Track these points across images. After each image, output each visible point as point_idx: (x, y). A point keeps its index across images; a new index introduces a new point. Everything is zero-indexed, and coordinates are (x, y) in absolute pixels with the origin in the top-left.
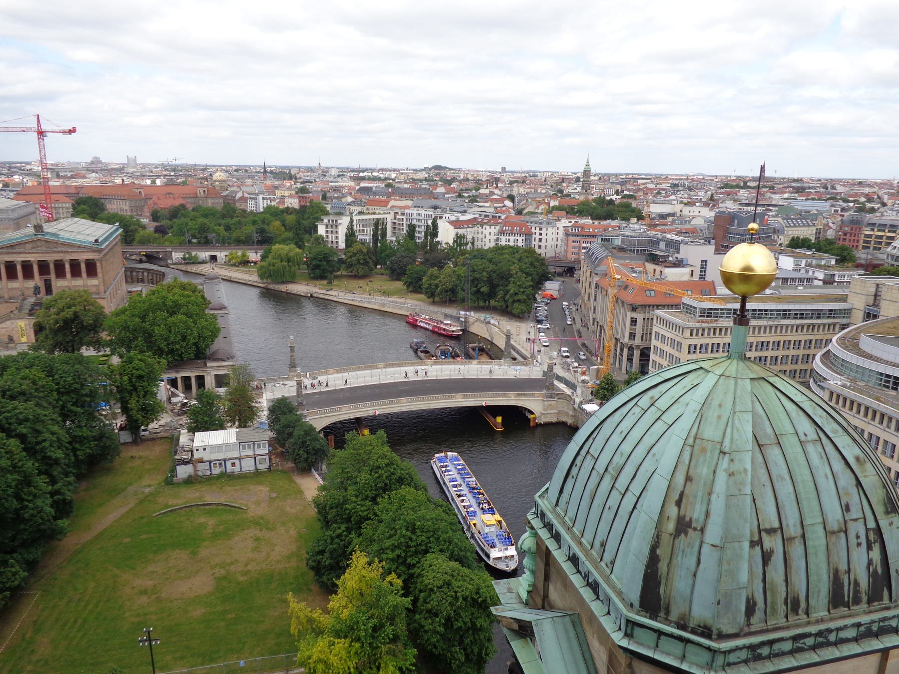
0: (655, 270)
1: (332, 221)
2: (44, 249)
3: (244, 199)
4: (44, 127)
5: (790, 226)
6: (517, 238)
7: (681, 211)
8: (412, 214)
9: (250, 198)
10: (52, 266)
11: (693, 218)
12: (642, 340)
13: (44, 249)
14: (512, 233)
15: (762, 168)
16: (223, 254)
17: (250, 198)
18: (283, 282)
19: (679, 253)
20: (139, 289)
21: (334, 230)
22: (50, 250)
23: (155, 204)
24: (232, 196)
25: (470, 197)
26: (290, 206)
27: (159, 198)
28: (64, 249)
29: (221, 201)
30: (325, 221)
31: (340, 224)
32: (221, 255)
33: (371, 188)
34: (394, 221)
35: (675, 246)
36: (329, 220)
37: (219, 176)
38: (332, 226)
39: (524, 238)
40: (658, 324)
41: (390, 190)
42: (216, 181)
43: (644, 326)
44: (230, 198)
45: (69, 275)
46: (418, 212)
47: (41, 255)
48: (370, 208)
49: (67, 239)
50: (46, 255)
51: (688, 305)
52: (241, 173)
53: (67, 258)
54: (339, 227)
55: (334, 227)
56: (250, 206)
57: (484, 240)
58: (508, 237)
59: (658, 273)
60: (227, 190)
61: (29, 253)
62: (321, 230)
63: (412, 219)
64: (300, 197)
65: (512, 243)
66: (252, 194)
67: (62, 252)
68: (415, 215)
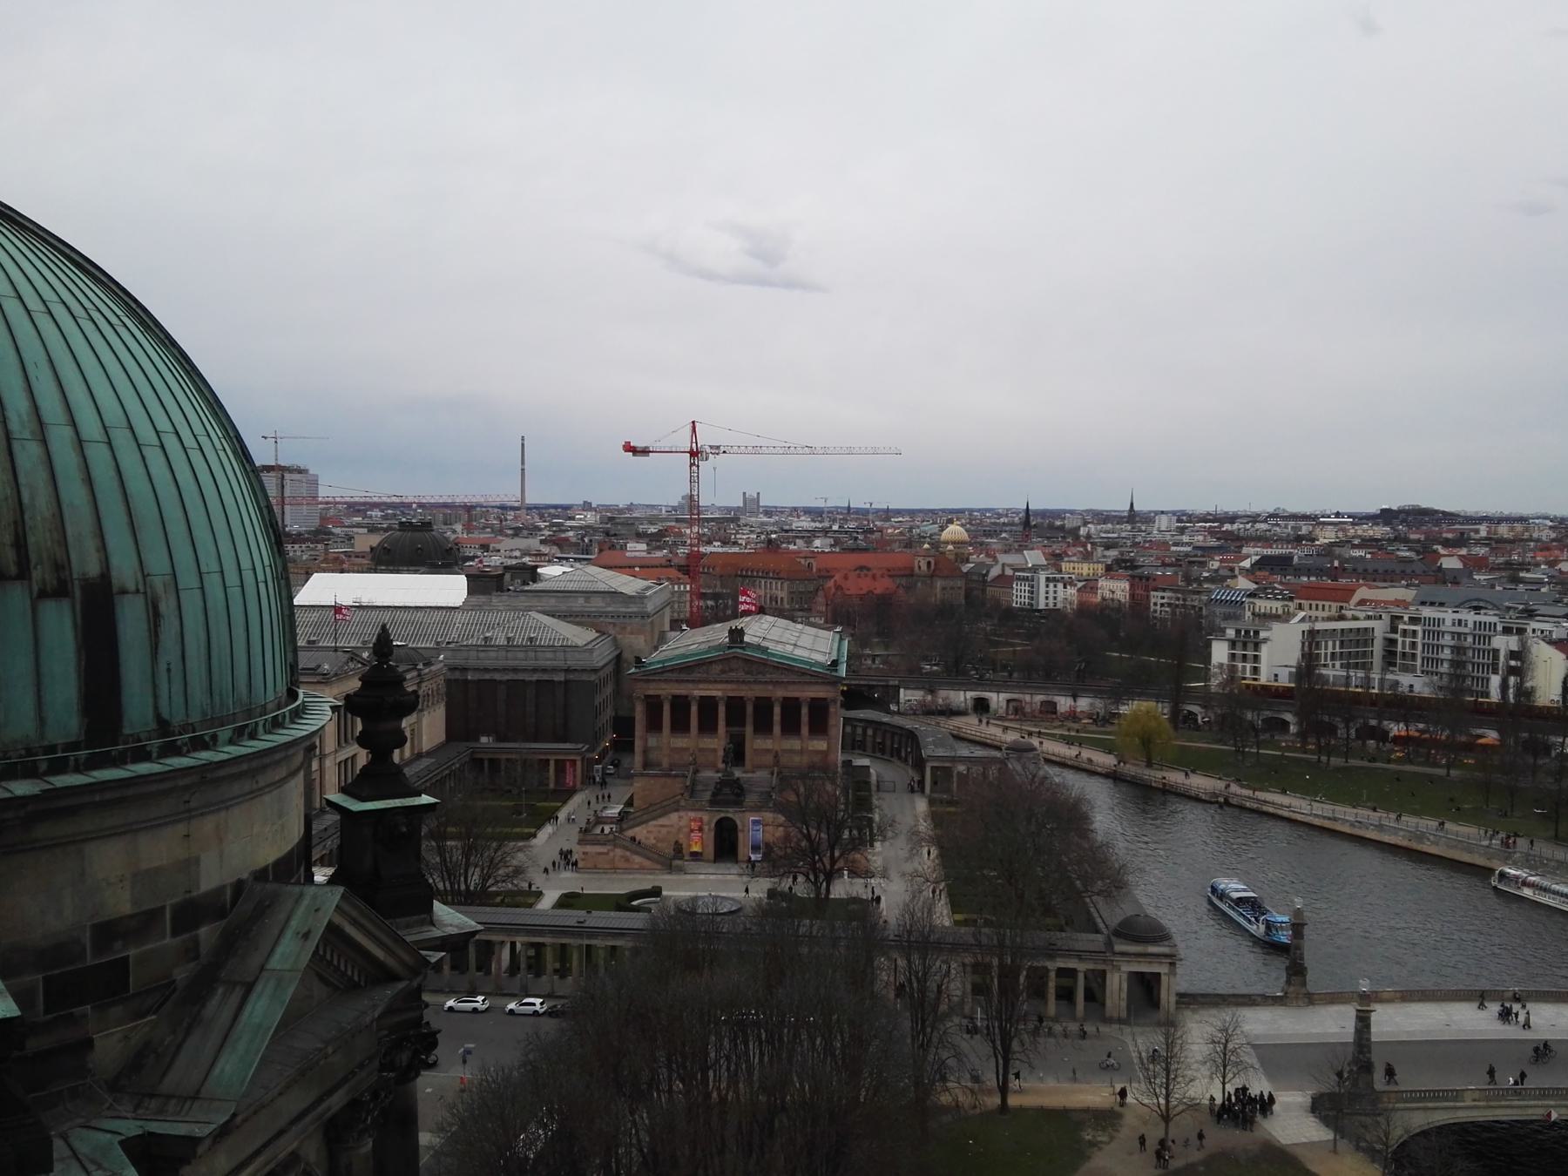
1: (1247, 632)
2: (741, 675)
3: (1004, 581)
4: (704, 440)
8: (1440, 622)
9: (1019, 578)
10: (750, 709)
13: (741, 675)
16: (1003, 697)
17: (1019, 578)
18: (1149, 765)
20: (865, 762)
21: (1250, 653)
22: (750, 678)
23: (838, 587)
24: (981, 574)
26: (1108, 595)
27: (846, 578)
28: (775, 677)
29: (960, 583)
31: (1265, 640)
32: (997, 699)
33: (1289, 558)
36: (1238, 632)
37: (955, 531)
41: (1336, 564)
42: (947, 543)
44: (975, 578)
45: (777, 729)
46: (1457, 616)
47: (734, 686)
48: (1305, 603)
49: (782, 657)
50: (743, 687)
52: (984, 526)
53: (780, 693)
54: (1264, 649)
55: (1250, 646)
56: (1019, 596)
60: (968, 561)
61: (716, 682)
62: (1220, 652)
63: (1440, 634)
64: (1133, 577)
66: (1023, 570)
67: (771, 682)
68: (1448, 622)
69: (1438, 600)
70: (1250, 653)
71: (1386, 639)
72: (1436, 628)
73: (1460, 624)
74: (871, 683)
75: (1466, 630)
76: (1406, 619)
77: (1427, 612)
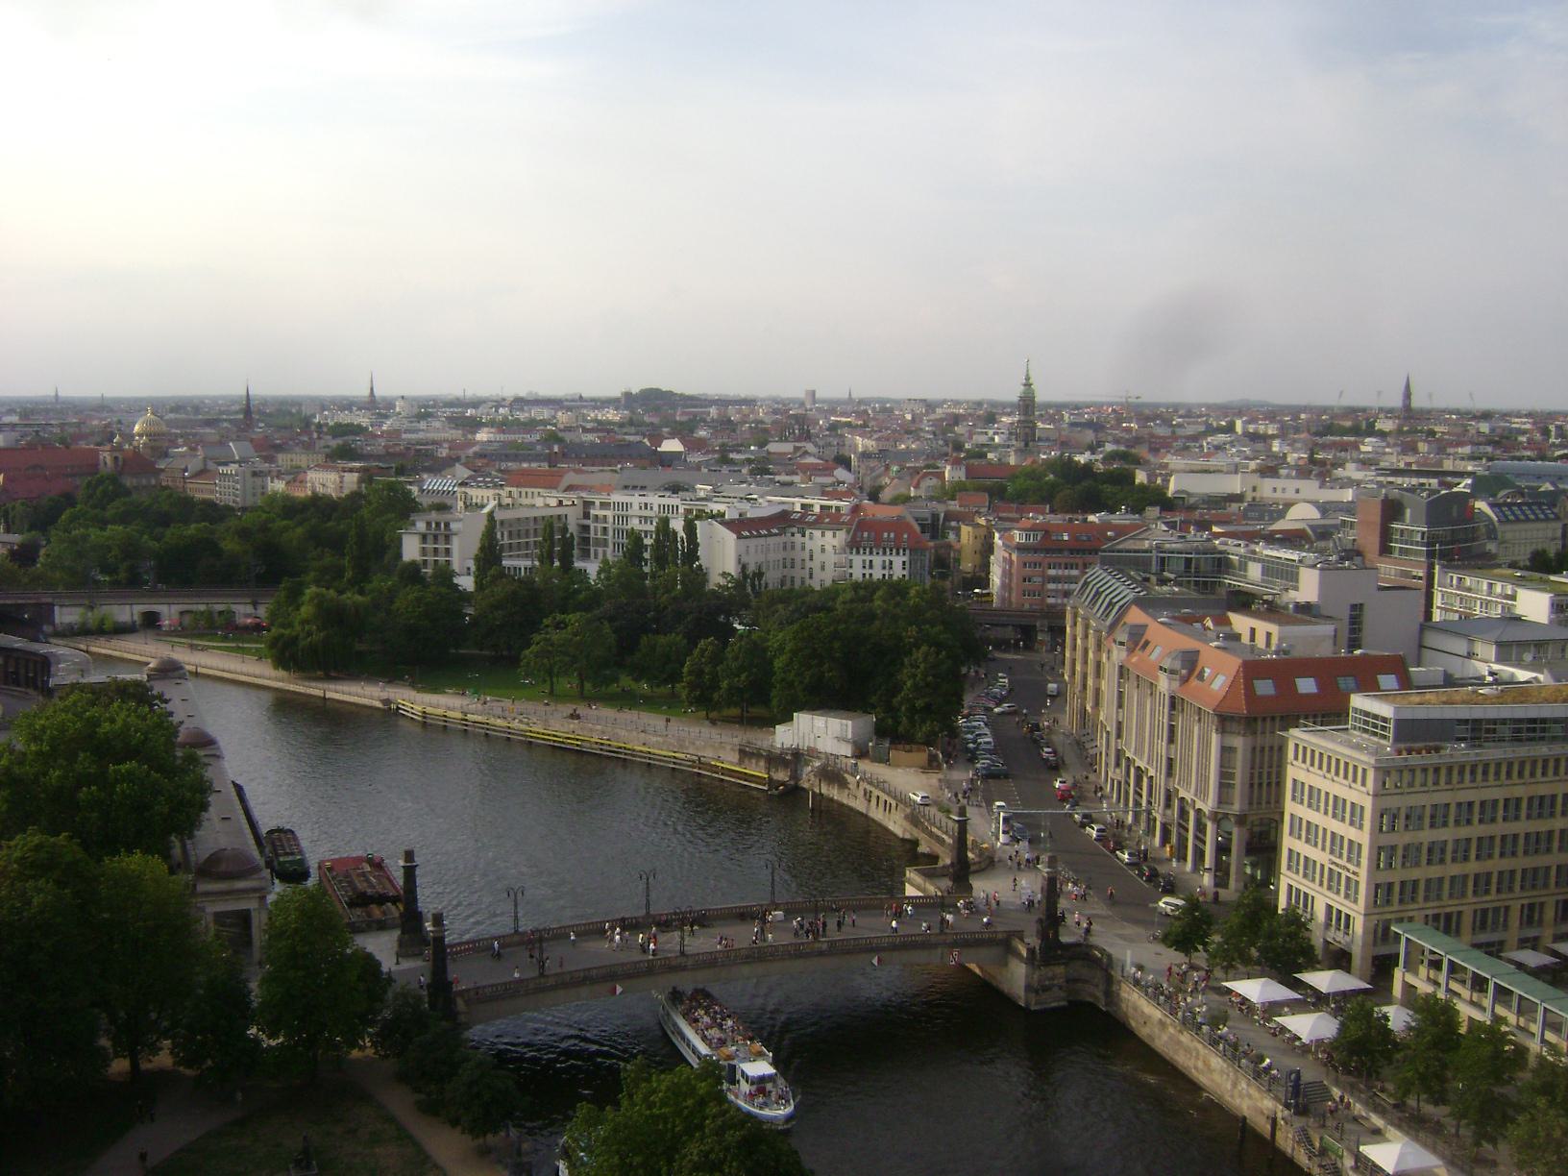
0: (1253, 631)
1: (438, 524)
5: (1508, 521)
6: (887, 558)
7: (1254, 489)
8: (627, 506)
11: (1288, 505)
12: (1251, 804)
14: (878, 545)
15: (1408, 394)
19: (1296, 589)
21: (441, 546)
25: (749, 461)
26: (320, 490)
30: (421, 526)
34: (586, 522)
35: (1288, 574)
36: (429, 524)
38: (436, 538)
39: (905, 559)
40: (1299, 763)
43: (1252, 768)
46: (643, 500)
51: (1367, 714)
54: (455, 540)
55: (441, 539)
57: (808, 564)
58: (868, 558)
59: (1261, 642)
62: (411, 549)
65: (877, 574)
69: (640, 484)
70: (441, 546)
71: (578, 525)
72: (624, 513)
73: (646, 508)
74: (20, 602)
75: (652, 514)
76: (597, 503)
77: (617, 497)
